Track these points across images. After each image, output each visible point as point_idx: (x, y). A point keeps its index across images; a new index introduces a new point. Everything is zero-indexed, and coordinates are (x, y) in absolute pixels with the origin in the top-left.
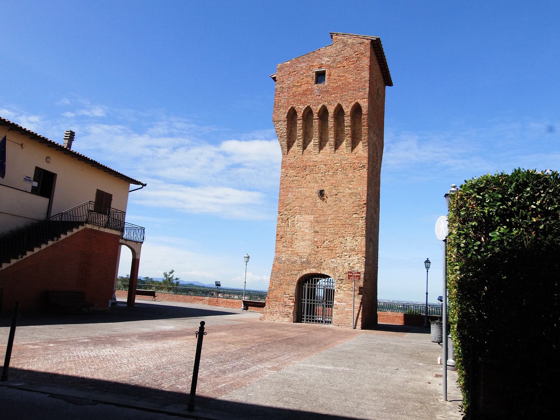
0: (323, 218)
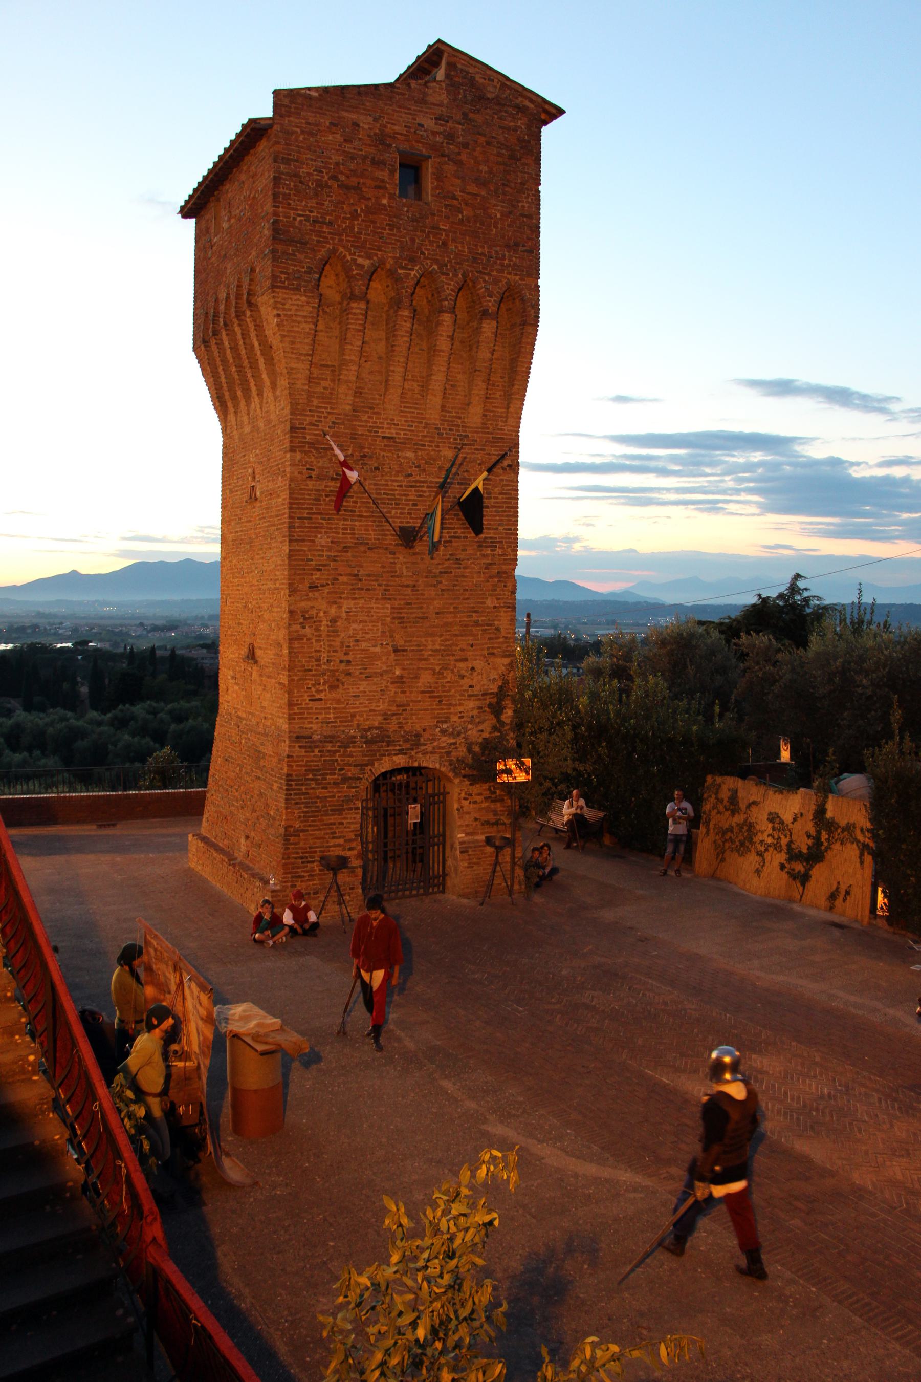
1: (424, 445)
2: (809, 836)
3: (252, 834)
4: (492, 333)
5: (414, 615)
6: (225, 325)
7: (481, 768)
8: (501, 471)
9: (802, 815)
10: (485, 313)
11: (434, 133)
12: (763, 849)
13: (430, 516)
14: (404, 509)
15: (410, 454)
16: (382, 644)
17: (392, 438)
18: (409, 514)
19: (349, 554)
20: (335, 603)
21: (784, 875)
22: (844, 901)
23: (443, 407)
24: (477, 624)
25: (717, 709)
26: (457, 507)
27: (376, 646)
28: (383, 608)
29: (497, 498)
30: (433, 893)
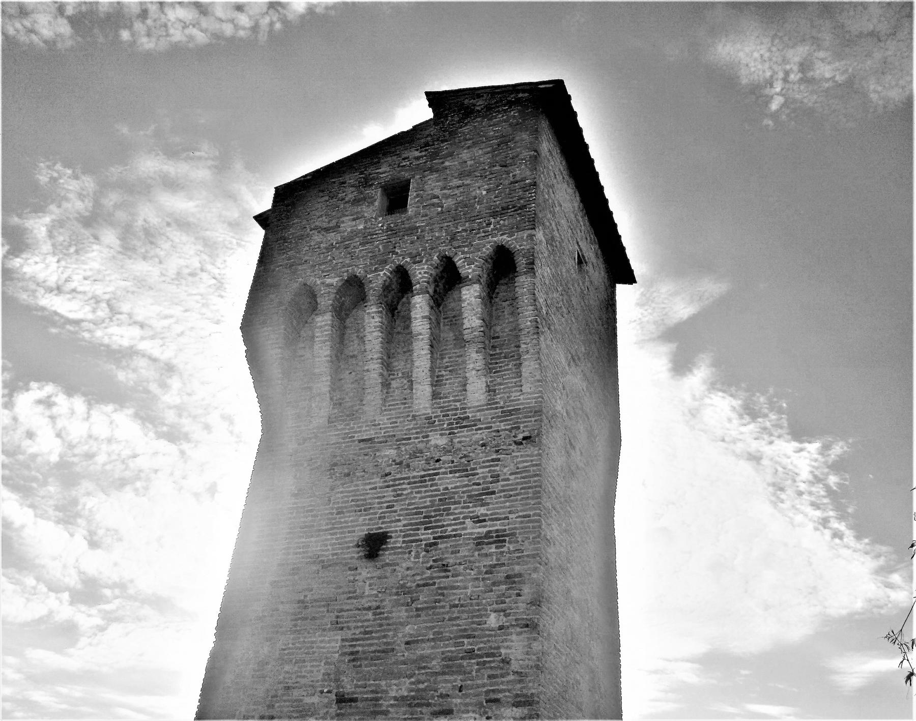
0: (375, 644)
1: (410, 439)
4: (476, 297)
5: (373, 648)
8: (514, 447)
11: (417, 158)
14: (375, 513)
15: (392, 452)
16: (322, 692)
17: (370, 439)
18: (380, 518)
23: (435, 395)
24: (470, 654)
27: (314, 695)
28: (329, 642)
29: (508, 480)
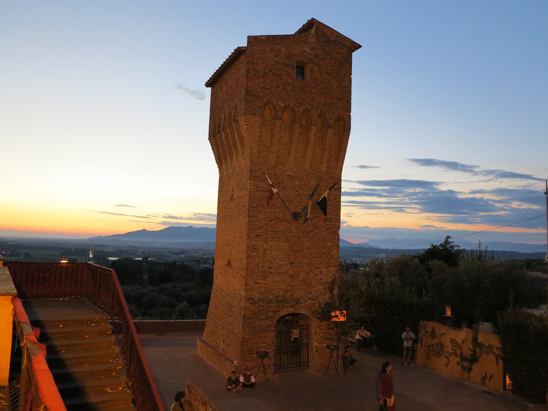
2: (470, 350)
3: (226, 340)
6: (223, 129)
7: (325, 314)
9: (466, 340)
10: (329, 126)
11: (310, 54)
12: (448, 355)
13: (306, 208)
15: (298, 183)
19: (272, 223)
20: (266, 243)
21: (459, 367)
22: (490, 380)
23: (311, 164)
25: (424, 292)
26: (316, 205)
30: (303, 369)
